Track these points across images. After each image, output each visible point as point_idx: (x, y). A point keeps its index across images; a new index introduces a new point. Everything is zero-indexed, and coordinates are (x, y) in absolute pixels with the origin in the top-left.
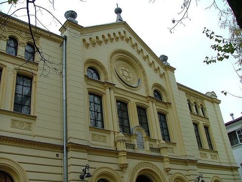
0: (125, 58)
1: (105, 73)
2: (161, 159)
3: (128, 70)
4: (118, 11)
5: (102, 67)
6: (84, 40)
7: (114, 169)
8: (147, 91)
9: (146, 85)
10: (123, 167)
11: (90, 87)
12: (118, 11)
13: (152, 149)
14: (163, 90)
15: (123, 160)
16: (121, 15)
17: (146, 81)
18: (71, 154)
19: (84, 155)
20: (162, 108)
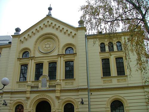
0: (48, 37)
1: (31, 52)
2: (54, 91)
3: (49, 43)
4: (50, 9)
5: (29, 50)
6: (21, 40)
7: (23, 100)
8: (59, 51)
9: (59, 48)
10: (28, 98)
11: (21, 62)
12: (50, 9)
13: (50, 87)
14: (73, 45)
15: (28, 95)
16: (51, 11)
17: (59, 45)
18: (4, 95)
19: (9, 95)
20: (68, 59)
